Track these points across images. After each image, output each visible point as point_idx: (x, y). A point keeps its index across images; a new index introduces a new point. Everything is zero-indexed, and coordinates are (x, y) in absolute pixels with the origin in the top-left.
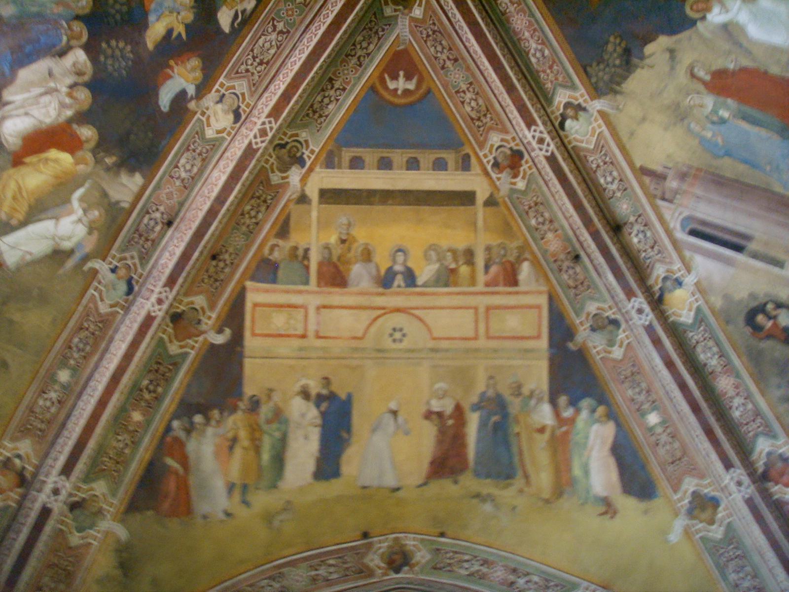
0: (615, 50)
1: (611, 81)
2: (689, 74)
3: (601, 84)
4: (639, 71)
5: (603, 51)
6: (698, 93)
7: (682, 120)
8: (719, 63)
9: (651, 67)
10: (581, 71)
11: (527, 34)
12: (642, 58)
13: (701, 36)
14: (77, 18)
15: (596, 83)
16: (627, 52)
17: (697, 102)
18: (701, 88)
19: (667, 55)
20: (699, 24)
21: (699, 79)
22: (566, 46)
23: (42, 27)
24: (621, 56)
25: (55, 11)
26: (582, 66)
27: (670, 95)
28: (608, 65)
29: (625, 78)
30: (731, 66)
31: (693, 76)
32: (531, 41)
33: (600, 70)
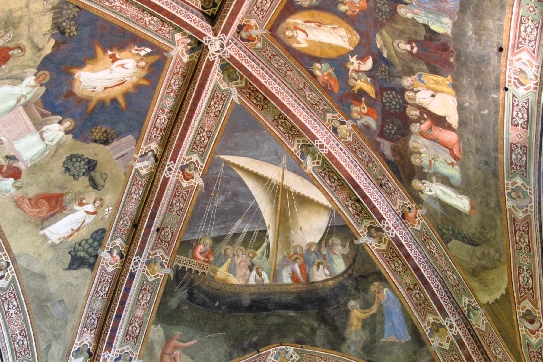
0: (70, 29)
1: (61, 12)
2: (21, 46)
3: (66, 7)
4: (50, 28)
5: (76, 24)
6: (9, 42)
7: (6, 22)
8: (11, 63)
9: (44, 35)
10: (81, 6)
11: (124, 7)
12: (53, 36)
13: (30, 67)
14: (406, 4)
15: (68, 5)
16: (63, 33)
17: (6, 38)
18: (10, 45)
19: (40, 47)
20: (36, 71)
21: (14, 49)
22: (98, 14)
23: (427, 6)
24: (65, 29)
25: (419, 11)
26: (83, 9)
27: (23, 29)
28: (68, 19)
29: (54, 19)
30: (3, 67)
31: (19, 48)
32: (120, 5)
33: (71, 13)
